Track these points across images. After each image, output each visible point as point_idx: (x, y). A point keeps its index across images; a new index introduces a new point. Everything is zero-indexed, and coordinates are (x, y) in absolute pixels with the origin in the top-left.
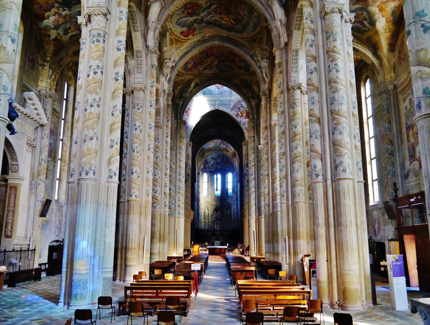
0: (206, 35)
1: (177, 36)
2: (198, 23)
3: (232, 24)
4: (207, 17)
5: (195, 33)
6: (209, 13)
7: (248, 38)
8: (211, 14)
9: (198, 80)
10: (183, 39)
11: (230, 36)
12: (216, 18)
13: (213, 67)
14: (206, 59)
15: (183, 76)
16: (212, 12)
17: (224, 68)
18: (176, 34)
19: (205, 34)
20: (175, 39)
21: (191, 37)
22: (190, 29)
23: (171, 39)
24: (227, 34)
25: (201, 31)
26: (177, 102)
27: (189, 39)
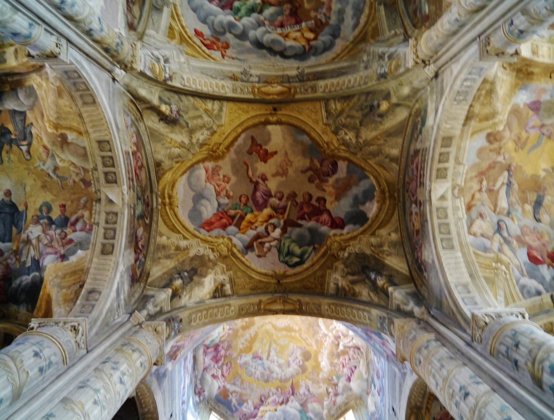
0: (253, 72)
1: (186, 32)
2: (237, 36)
3: (308, 40)
5: (229, 52)
6: (260, 24)
7: (347, 47)
8: (264, 25)
9: (227, 278)
10: (198, 46)
11: (307, 71)
13: (269, 249)
14: (252, 212)
15: (185, 238)
16: (267, 23)
17: (297, 250)
18: (184, 24)
19: (250, 67)
20: (181, 34)
21: (217, 54)
23: (171, 28)
24: (298, 68)
25: (241, 57)
26: (150, 293)
27: (213, 59)
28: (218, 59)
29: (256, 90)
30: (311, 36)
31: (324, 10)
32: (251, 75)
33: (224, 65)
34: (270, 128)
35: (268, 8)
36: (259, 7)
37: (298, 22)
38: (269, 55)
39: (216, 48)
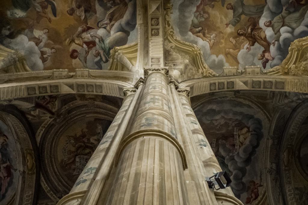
0: (269, 166)
2: (244, 175)
3: (248, 131)
4: (236, 162)
5: (257, 181)
6: (232, 159)
7: (265, 113)
11: (272, 134)
12: (241, 151)
16: (231, 154)
19: (266, 168)
21: (261, 190)
22: (249, 188)
27: (265, 193)
28: (264, 189)
29: (287, 168)
30: (245, 130)
31: (230, 122)
32: (271, 168)
33: (267, 186)
34: (301, 155)
35: (221, 153)
36: (220, 158)
37: (233, 136)
38: (256, 155)
39: (256, 190)
